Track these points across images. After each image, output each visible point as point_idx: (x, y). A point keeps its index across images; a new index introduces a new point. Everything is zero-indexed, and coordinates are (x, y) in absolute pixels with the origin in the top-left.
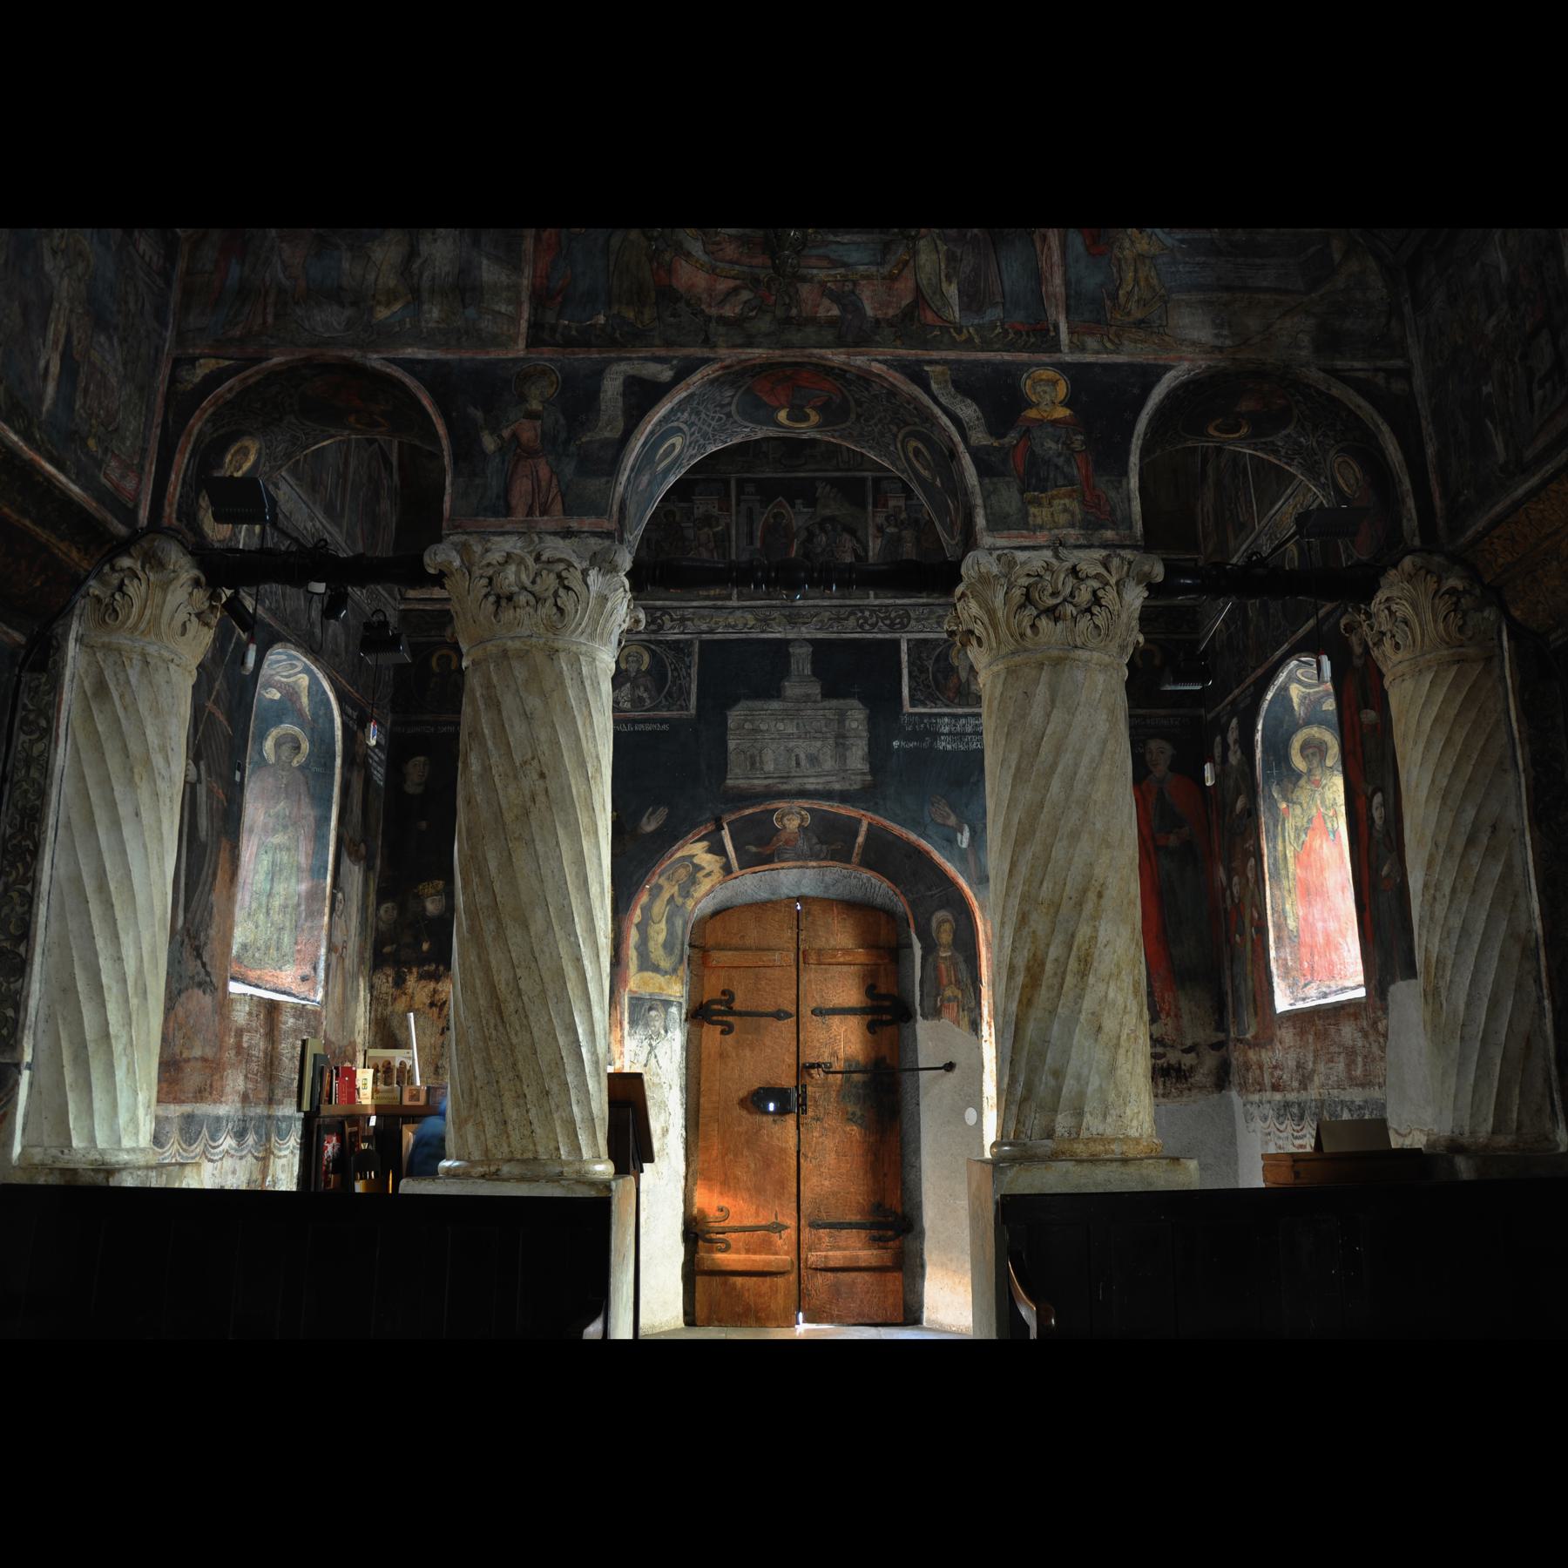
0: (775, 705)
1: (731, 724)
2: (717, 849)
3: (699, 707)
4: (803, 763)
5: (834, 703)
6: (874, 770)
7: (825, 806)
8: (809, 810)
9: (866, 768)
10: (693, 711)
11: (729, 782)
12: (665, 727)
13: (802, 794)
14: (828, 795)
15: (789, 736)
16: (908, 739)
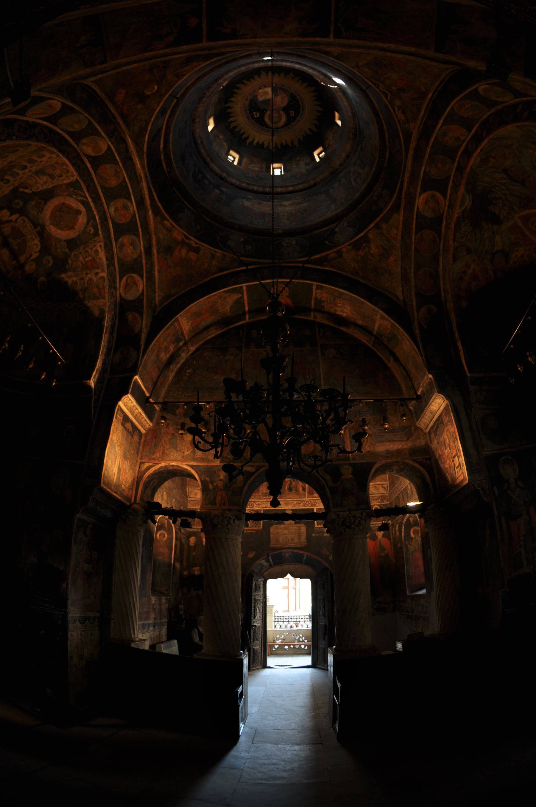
0: (282, 526)
1: (271, 531)
2: (268, 561)
3: (263, 526)
4: (290, 540)
5: (298, 525)
6: (308, 542)
7: (295, 551)
8: (292, 552)
9: (306, 541)
10: (261, 527)
11: (271, 545)
12: (254, 532)
13: (290, 548)
14: (296, 548)
15: (286, 534)
16: (316, 533)
